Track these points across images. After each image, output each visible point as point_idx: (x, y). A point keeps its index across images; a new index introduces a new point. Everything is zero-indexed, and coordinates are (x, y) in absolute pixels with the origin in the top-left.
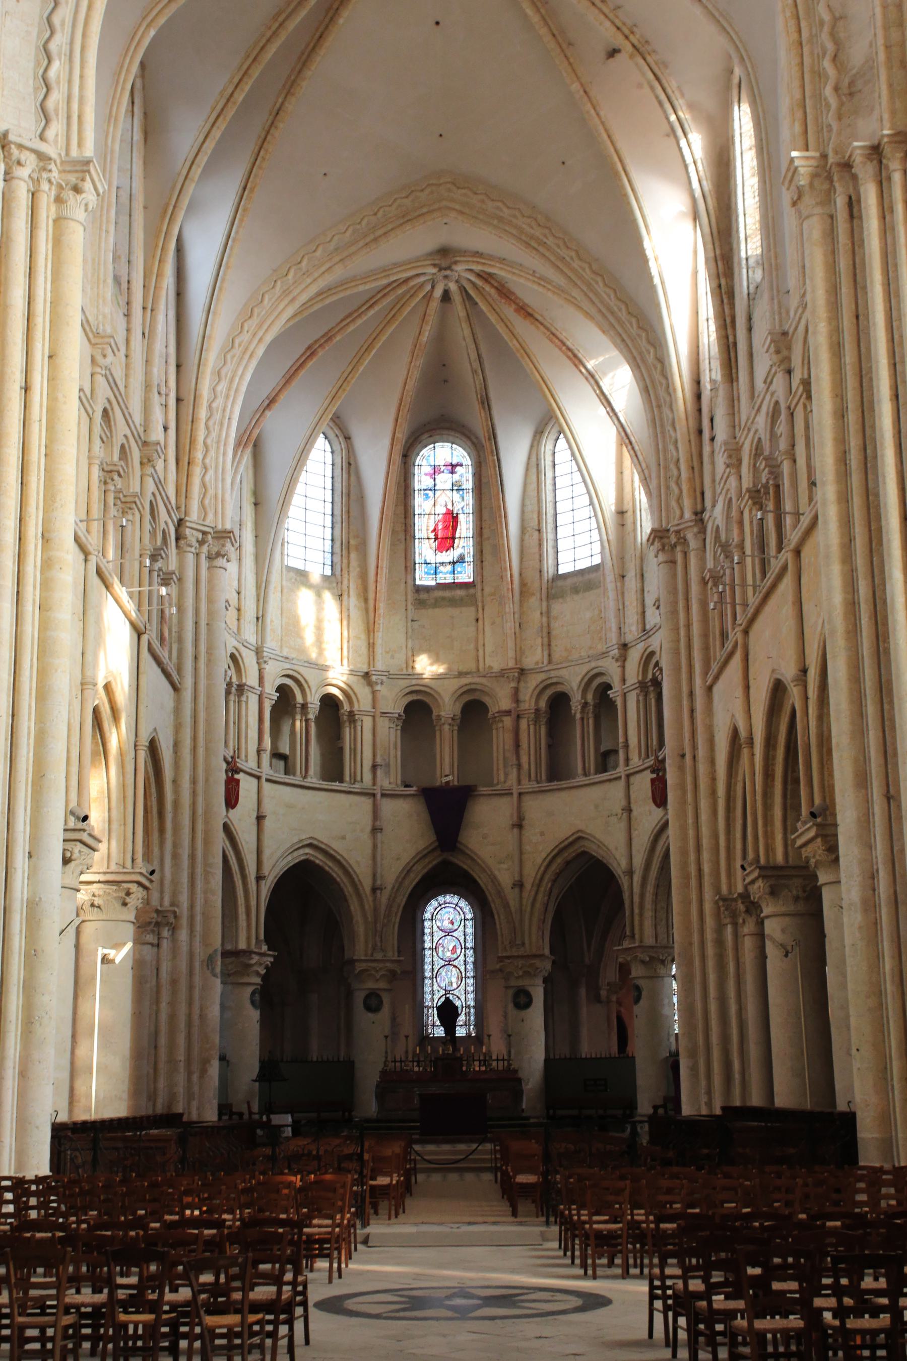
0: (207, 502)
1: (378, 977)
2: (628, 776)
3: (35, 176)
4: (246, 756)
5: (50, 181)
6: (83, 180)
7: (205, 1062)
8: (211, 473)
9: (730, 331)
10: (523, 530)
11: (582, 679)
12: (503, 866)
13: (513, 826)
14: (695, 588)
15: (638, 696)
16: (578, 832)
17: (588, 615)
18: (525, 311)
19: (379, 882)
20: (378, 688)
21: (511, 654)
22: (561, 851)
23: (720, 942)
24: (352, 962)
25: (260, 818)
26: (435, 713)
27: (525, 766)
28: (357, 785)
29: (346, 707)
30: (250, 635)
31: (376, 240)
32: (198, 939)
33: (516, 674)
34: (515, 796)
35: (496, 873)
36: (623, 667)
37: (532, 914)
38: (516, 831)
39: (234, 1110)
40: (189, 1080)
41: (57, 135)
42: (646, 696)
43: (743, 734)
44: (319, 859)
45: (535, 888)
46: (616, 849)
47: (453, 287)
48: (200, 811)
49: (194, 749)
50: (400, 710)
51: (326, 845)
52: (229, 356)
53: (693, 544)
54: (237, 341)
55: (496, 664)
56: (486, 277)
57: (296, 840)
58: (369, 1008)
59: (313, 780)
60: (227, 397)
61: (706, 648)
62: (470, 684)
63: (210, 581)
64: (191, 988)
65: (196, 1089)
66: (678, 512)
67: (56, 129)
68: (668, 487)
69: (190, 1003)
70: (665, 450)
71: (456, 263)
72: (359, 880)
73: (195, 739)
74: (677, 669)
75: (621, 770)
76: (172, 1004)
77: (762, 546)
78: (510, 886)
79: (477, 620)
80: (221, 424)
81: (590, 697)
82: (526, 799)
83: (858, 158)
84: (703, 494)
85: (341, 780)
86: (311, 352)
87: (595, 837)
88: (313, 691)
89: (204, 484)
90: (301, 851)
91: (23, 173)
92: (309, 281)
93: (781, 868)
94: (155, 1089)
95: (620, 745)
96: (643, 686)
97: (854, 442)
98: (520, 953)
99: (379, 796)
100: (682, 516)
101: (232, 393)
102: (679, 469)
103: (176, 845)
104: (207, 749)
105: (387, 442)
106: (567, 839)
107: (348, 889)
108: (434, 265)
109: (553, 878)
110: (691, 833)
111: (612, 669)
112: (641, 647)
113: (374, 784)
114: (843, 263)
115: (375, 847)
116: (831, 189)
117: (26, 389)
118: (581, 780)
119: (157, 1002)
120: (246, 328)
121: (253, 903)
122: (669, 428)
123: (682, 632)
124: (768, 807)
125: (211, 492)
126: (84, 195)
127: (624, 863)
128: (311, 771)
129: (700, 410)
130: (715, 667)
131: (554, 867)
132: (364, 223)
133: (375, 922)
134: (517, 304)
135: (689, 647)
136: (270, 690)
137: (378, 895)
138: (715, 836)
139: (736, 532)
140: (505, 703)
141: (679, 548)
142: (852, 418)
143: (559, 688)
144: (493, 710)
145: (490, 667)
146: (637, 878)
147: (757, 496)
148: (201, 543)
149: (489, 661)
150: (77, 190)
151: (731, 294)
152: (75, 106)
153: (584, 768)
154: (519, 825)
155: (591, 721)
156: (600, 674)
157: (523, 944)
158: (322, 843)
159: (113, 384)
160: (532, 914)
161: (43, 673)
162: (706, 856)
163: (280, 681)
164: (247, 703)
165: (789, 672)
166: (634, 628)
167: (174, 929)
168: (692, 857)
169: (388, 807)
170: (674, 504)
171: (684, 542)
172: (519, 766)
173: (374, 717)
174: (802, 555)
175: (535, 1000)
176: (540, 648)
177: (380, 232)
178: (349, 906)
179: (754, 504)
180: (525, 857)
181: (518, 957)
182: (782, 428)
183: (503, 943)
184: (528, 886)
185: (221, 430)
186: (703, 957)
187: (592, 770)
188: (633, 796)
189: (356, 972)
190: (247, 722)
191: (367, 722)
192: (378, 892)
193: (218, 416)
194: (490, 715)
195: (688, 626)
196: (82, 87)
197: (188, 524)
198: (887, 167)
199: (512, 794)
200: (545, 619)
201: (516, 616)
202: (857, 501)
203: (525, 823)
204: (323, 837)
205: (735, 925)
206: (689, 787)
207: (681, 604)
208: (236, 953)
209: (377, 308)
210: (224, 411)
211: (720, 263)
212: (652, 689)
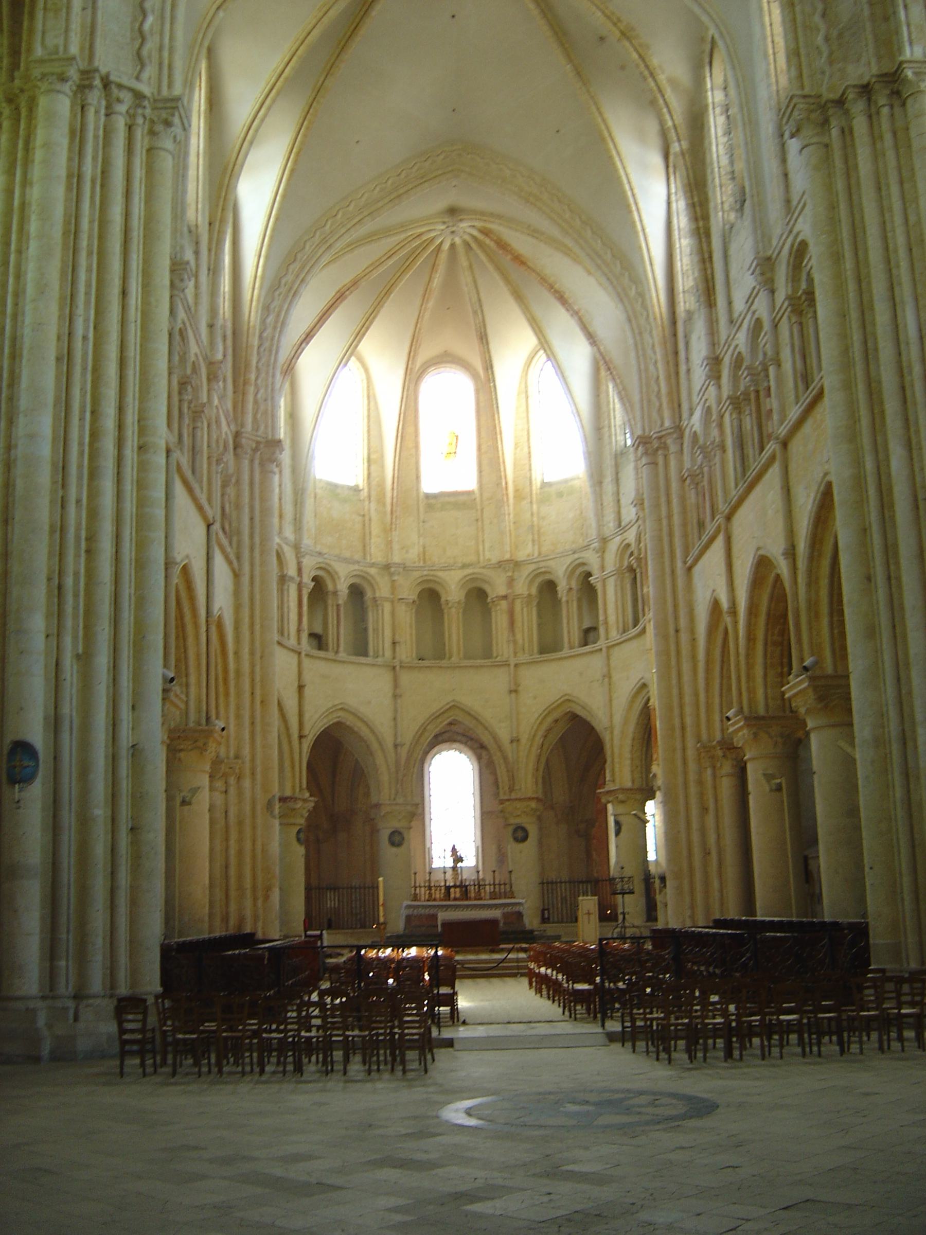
0: (259, 416)
3: (132, 111)
4: (289, 635)
5: (144, 117)
6: (173, 115)
7: (268, 889)
8: (262, 391)
9: (708, 265)
10: (516, 446)
11: (568, 567)
13: (511, 692)
14: (674, 485)
15: (616, 581)
16: (566, 695)
17: (571, 515)
18: (519, 260)
19: (399, 740)
20: (396, 578)
21: (507, 548)
22: (549, 713)
23: (700, 783)
24: (377, 806)
25: (301, 688)
26: (443, 600)
27: (520, 642)
28: (380, 660)
29: (369, 595)
30: (289, 533)
31: (399, 196)
32: (258, 787)
33: (512, 565)
36: (602, 558)
40: (255, 905)
41: (150, 78)
42: (622, 581)
43: (725, 604)
44: (350, 720)
47: (458, 240)
48: (258, 679)
49: (252, 625)
50: (414, 596)
52: (277, 293)
53: (673, 448)
54: (283, 281)
55: (493, 556)
56: (486, 232)
58: (393, 843)
59: (342, 655)
60: (275, 328)
61: (685, 535)
62: (473, 574)
63: (262, 483)
64: (254, 828)
65: (261, 912)
66: (659, 423)
67: (149, 72)
68: (649, 401)
69: (254, 842)
70: (647, 370)
71: (461, 220)
73: (252, 617)
74: (661, 554)
75: (602, 643)
76: (240, 840)
77: (741, 445)
79: (477, 520)
80: (270, 351)
81: (574, 584)
83: (851, 96)
84: (680, 406)
85: (365, 654)
86: (340, 297)
88: (343, 580)
89: (256, 402)
90: (335, 715)
91: (123, 108)
92: (343, 230)
93: (763, 718)
94: (227, 913)
95: (601, 623)
96: (619, 573)
97: (856, 337)
100: (662, 424)
101: (279, 325)
102: (659, 385)
103: (238, 708)
104: (262, 626)
105: (401, 372)
107: (375, 746)
108: (444, 223)
110: (675, 691)
111: (592, 559)
112: (618, 540)
113: (394, 658)
114: (840, 185)
115: (396, 711)
116: (826, 122)
117: (124, 293)
118: (566, 652)
119: (227, 840)
120: (290, 270)
121: (297, 757)
122: (649, 352)
123: (665, 522)
124: (750, 666)
125: (262, 408)
126: (173, 129)
128: (341, 649)
129: (675, 335)
130: (695, 552)
131: (545, 726)
132: (390, 182)
133: (397, 772)
134: (512, 254)
135: (671, 534)
136: (307, 580)
138: (696, 694)
139: (715, 433)
140: (502, 590)
141: (660, 452)
142: (854, 315)
143: (547, 577)
144: (492, 595)
145: (489, 560)
146: (617, 732)
147: (737, 403)
148: (255, 450)
149: (488, 555)
150: (168, 124)
151: (708, 235)
152: (166, 54)
153: (569, 642)
154: (516, 691)
155: (575, 604)
156: (584, 564)
159: (188, 309)
161: (141, 545)
162: (688, 710)
163: (313, 574)
164: (288, 590)
165: (776, 549)
166: (611, 525)
167: (239, 778)
168: (676, 711)
169: (406, 678)
170: (655, 415)
171: (665, 447)
172: (515, 642)
173: (392, 602)
174: (790, 446)
175: (530, 835)
176: (530, 544)
177: (401, 191)
179: (735, 408)
181: (516, 799)
182: (765, 338)
185: (270, 355)
186: (686, 797)
187: (577, 645)
188: (613, 664)
190: (288, 607)
191: (387, 607)
192: (399, 748)
193: (267, 344)
194: (489, 600)
195: (670, 517)
196: (171, 39)
197: (244, 435)
198: (876, 102)
199: (509, 665)
200: (535, 519)
201: (512, 516)
202: (861, 387)
203: (520, 688)
205: (714, 767)
206: (673, 654)
207: (663, 499)
209: (395, 258)
210: (272, 339)
211: (698, 209)
212: (627, 575)
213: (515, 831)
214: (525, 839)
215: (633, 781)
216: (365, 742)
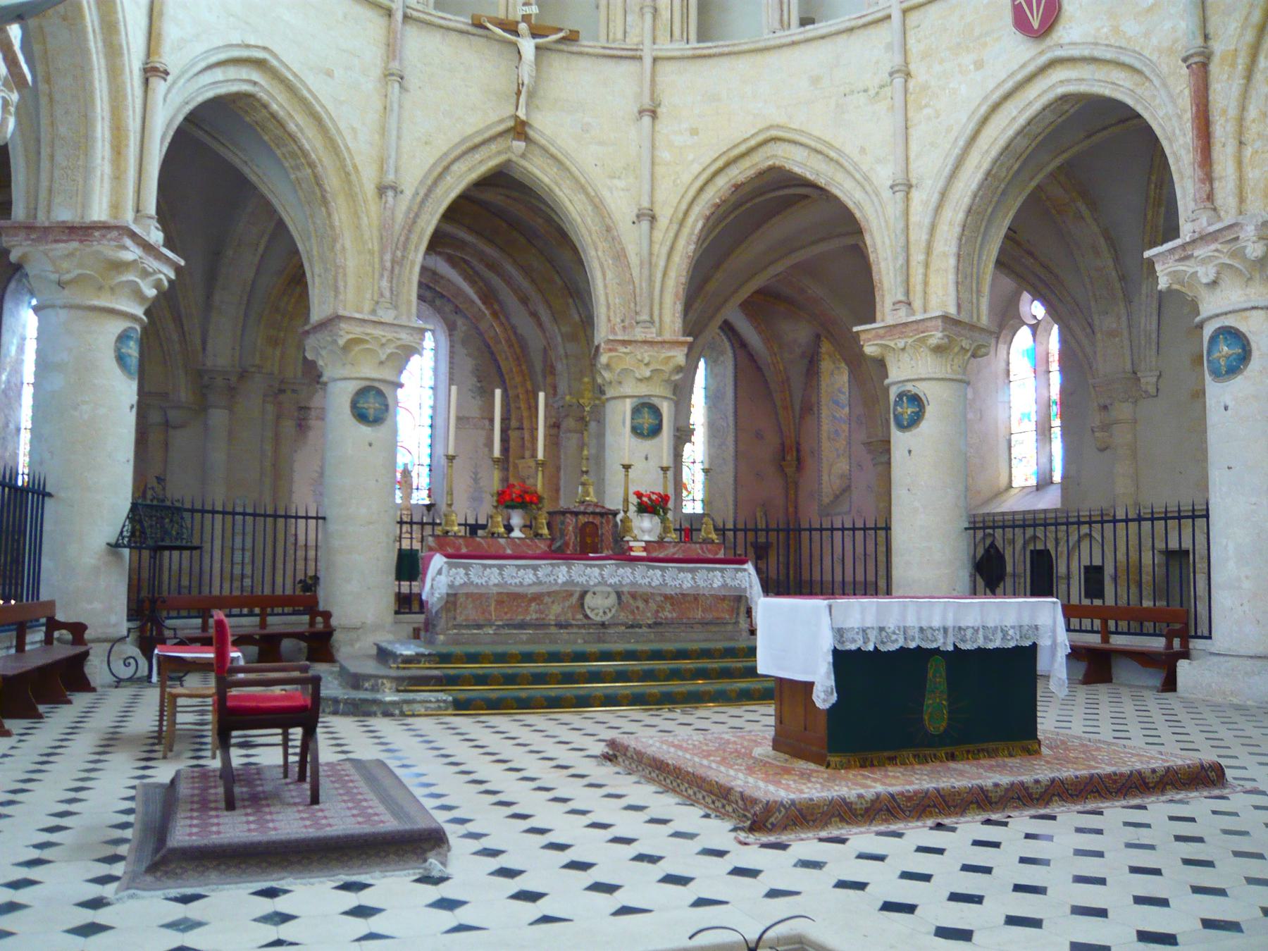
1: (383, 357)
2: (905, 12)
12: (616, 182)
13: (641, 112)
22: (727, 165)
34: (648, 61)
35: (606, 194)
37: (665, 274)
38: (647, 120)
39: (60, 617)
45: (675, 227)
46: (863, 150)
51: (295, 75)
57: (236, 39)
72: (355, 167)
78: (631, 214)
82: (666, 69)
87: (810, 135)
98: (649, 337)
99: (399, 16)
106: (745, 140)
107: (332, 182)
109: (708, 213)
121: (133, 124)
127: (884, 175)
137: (390, 199)
154: (654, 114)
157: (652, 322)
158: (288, 68)
160: (665, 274)
169: (417, 44)
178: (329, 215)
180: (660, 170)
181: (645, 342)
183: (609, 320)
184: (663, 222)
189: (341, 342)
192: (390, 193)
199: (640, 58)
203: (661, 111)
204: (291, 58)
208: (82, 231)
213: (636, 411)
214: (655, 431)
215: (959, 306)
216: (312, 165)
